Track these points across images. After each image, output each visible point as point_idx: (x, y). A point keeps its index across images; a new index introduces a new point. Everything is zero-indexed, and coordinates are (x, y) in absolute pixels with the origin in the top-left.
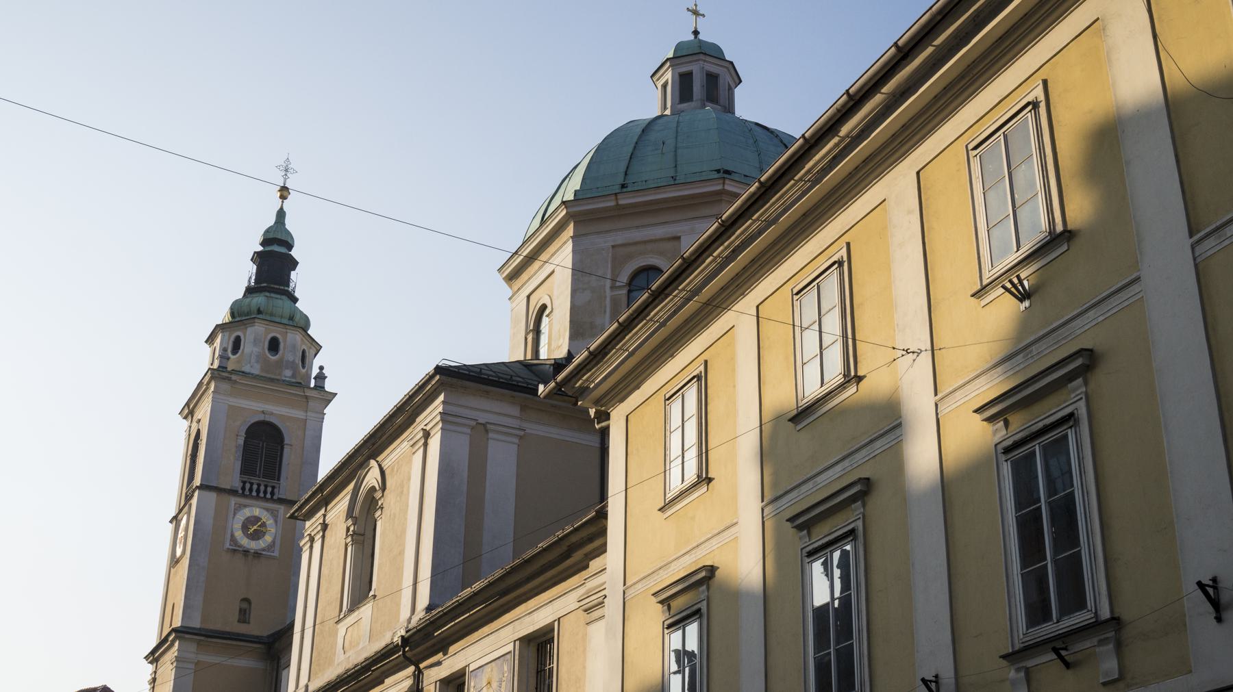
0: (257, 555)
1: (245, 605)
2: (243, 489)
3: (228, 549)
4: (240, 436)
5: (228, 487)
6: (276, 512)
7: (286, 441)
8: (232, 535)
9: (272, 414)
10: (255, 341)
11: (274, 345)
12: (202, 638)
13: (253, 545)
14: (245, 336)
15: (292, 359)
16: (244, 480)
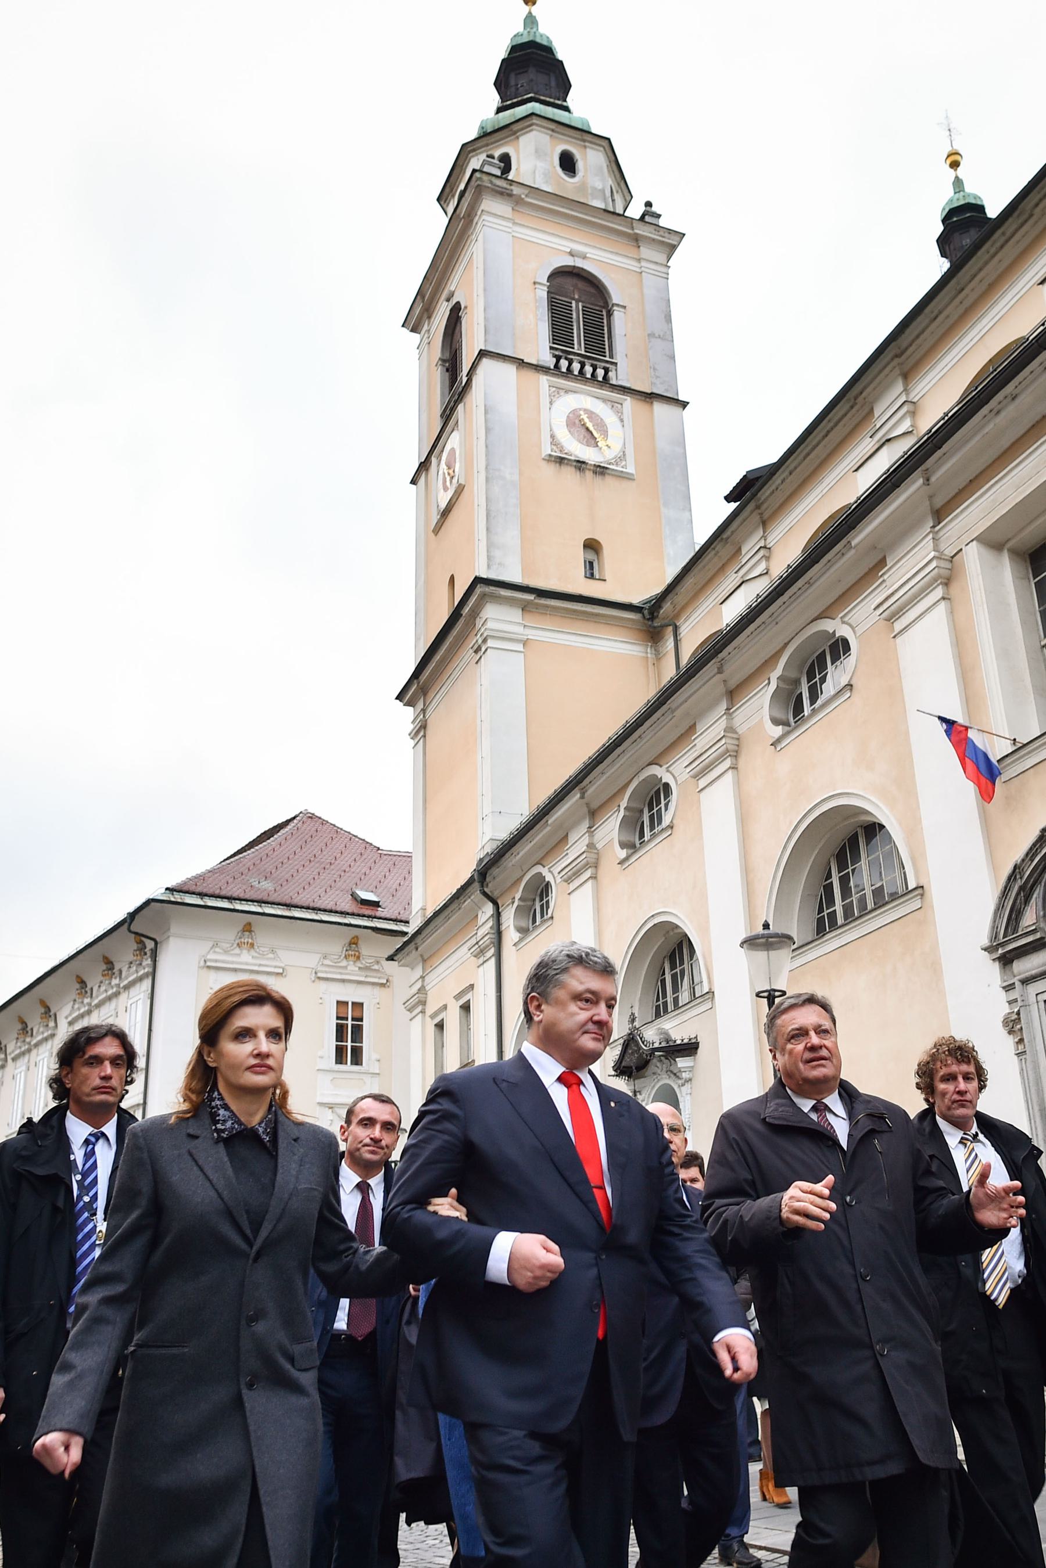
0: (600, 470)
1: (591, 556)
2: (557, 366)
3: (550, 455)
4: (540, 284)
5: (534, 362)
6: (619, 406)
7: (616, 297)
8: (553, 437)
9: (584, 257)
10: (537, 151)
11: (568, 163)
12: (530, 597)
13: (590, 455)
14: (517, 152)
15: (600, 187)
16: (557, 353)
